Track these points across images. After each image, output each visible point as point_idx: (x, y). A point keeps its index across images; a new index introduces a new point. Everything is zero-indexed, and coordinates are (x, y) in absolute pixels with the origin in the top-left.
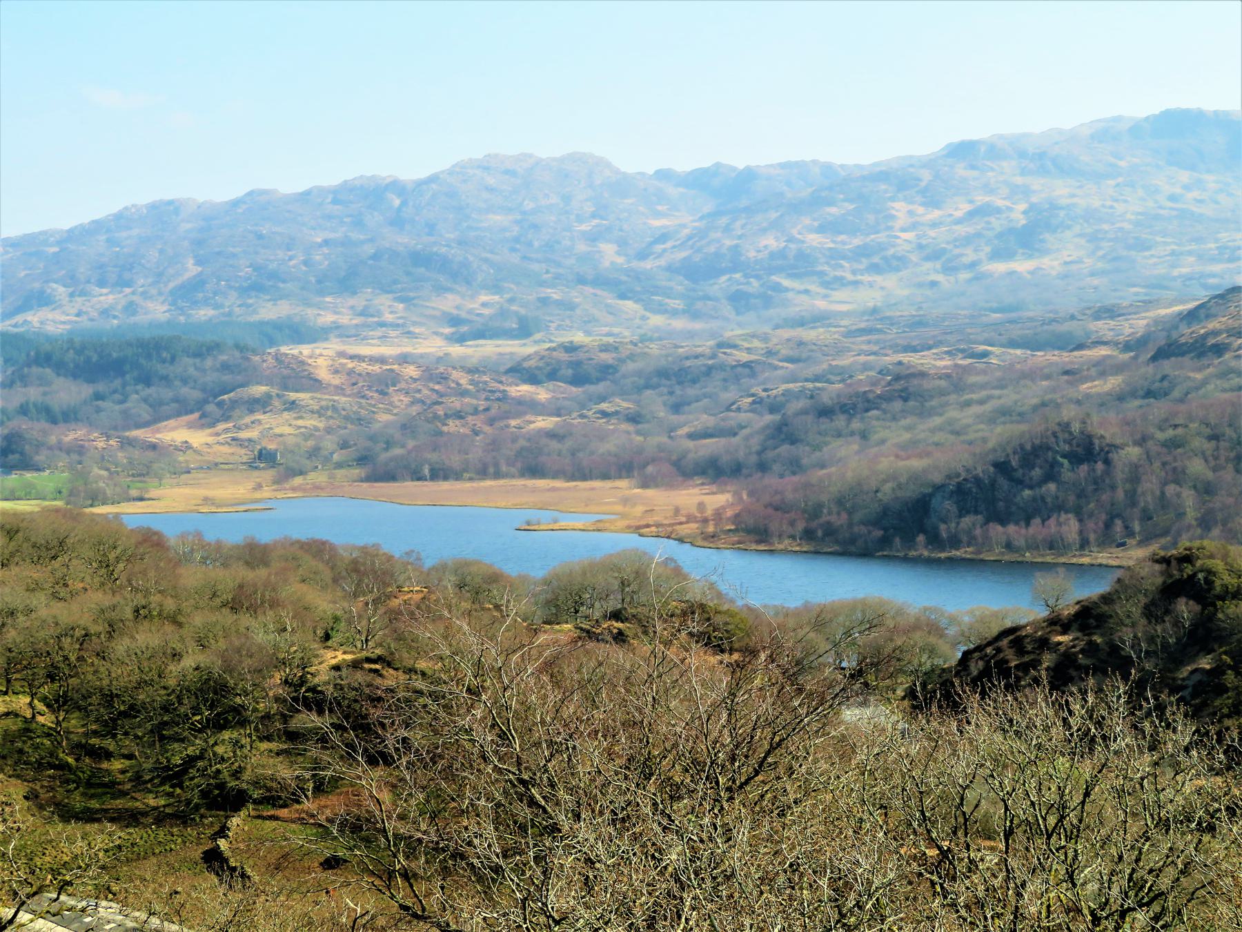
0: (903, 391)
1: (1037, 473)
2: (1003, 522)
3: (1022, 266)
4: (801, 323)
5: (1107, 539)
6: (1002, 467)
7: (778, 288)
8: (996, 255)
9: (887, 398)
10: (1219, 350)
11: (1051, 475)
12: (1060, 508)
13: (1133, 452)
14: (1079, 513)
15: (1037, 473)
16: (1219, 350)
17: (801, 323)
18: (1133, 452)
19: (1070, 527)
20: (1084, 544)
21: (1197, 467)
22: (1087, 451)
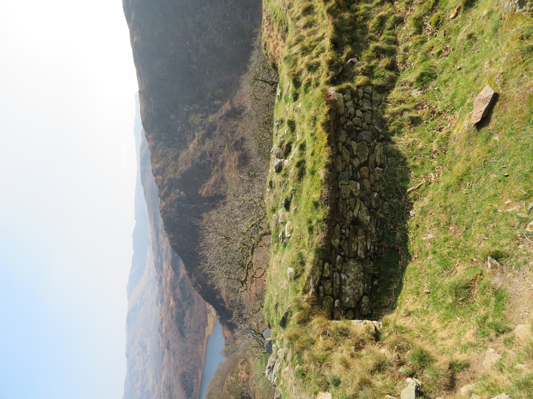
0: (169, 388)
1: (186, 384)
2: (193, 390)
3: (148, 349)
4: (153, 390)
5: (197, 375)
6: (185, 389)
7: (147, 391)
8: (146, 352)
9: (170, 391)
10: (169, 342)
11: (187, 381)
12: (192, 381)
13: (184, 368)
14: (193, 378)
15: (186, 384)
16: (169, 342)
17: (153, 390)
18: (184, 368)
19: (195, 380)
20: (198, 379)
21: (187, 360)
22: (183, 375)
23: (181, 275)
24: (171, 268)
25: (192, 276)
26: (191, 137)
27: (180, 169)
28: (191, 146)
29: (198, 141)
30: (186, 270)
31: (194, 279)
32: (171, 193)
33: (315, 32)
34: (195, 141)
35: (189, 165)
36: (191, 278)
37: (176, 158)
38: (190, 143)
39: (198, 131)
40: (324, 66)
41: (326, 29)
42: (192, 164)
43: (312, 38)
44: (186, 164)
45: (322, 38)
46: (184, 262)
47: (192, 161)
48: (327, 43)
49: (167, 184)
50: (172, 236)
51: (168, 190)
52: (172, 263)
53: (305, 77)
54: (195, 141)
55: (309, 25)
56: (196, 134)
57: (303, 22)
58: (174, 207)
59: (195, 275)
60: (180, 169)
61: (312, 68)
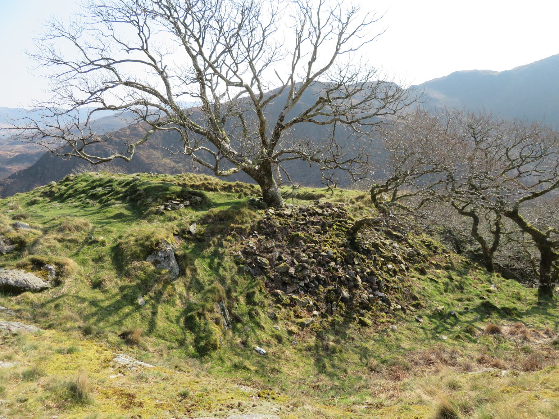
23: (9, 167)
24: (17, 154)
25: (12, 179)
26: (177, 160)
27: (141, 152)
28: (167, 161)
29: (174, 167)
30: (20, 171)
31: (8, 182)
32: (113, 145)
33: (198, 181)
34: (173, 164)
35: (146, 161)
36: (9, 178)
37: (152, 147)
38: (170, 159)
39: (184, 166)
40: (184, 182)
41: (198, 183)
42: (148, 164)
43: (196, 180)
44: (147, 158)
45: (195, 182)
46: (30, 168)
47: (151, 164)
48: (193, 183)
49: (122, 140)
50: (61, 151)
51: (116, 142)
52: (23, 155)
53: (181, 179)
54: (173, 164)
55: (201, 179)
56: (180, 164)
57: (202, 178)
58: (96, 150)
59: (14, 182)
60: (141, 152)
61: (184, 180)
